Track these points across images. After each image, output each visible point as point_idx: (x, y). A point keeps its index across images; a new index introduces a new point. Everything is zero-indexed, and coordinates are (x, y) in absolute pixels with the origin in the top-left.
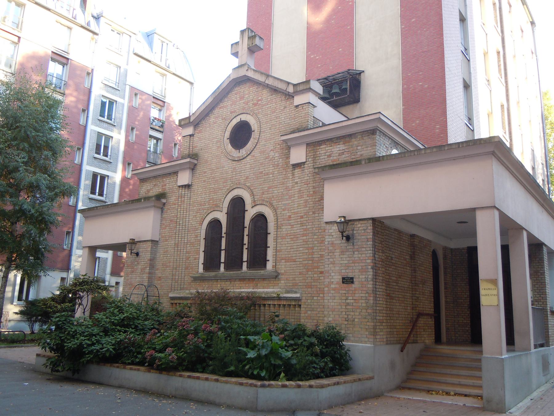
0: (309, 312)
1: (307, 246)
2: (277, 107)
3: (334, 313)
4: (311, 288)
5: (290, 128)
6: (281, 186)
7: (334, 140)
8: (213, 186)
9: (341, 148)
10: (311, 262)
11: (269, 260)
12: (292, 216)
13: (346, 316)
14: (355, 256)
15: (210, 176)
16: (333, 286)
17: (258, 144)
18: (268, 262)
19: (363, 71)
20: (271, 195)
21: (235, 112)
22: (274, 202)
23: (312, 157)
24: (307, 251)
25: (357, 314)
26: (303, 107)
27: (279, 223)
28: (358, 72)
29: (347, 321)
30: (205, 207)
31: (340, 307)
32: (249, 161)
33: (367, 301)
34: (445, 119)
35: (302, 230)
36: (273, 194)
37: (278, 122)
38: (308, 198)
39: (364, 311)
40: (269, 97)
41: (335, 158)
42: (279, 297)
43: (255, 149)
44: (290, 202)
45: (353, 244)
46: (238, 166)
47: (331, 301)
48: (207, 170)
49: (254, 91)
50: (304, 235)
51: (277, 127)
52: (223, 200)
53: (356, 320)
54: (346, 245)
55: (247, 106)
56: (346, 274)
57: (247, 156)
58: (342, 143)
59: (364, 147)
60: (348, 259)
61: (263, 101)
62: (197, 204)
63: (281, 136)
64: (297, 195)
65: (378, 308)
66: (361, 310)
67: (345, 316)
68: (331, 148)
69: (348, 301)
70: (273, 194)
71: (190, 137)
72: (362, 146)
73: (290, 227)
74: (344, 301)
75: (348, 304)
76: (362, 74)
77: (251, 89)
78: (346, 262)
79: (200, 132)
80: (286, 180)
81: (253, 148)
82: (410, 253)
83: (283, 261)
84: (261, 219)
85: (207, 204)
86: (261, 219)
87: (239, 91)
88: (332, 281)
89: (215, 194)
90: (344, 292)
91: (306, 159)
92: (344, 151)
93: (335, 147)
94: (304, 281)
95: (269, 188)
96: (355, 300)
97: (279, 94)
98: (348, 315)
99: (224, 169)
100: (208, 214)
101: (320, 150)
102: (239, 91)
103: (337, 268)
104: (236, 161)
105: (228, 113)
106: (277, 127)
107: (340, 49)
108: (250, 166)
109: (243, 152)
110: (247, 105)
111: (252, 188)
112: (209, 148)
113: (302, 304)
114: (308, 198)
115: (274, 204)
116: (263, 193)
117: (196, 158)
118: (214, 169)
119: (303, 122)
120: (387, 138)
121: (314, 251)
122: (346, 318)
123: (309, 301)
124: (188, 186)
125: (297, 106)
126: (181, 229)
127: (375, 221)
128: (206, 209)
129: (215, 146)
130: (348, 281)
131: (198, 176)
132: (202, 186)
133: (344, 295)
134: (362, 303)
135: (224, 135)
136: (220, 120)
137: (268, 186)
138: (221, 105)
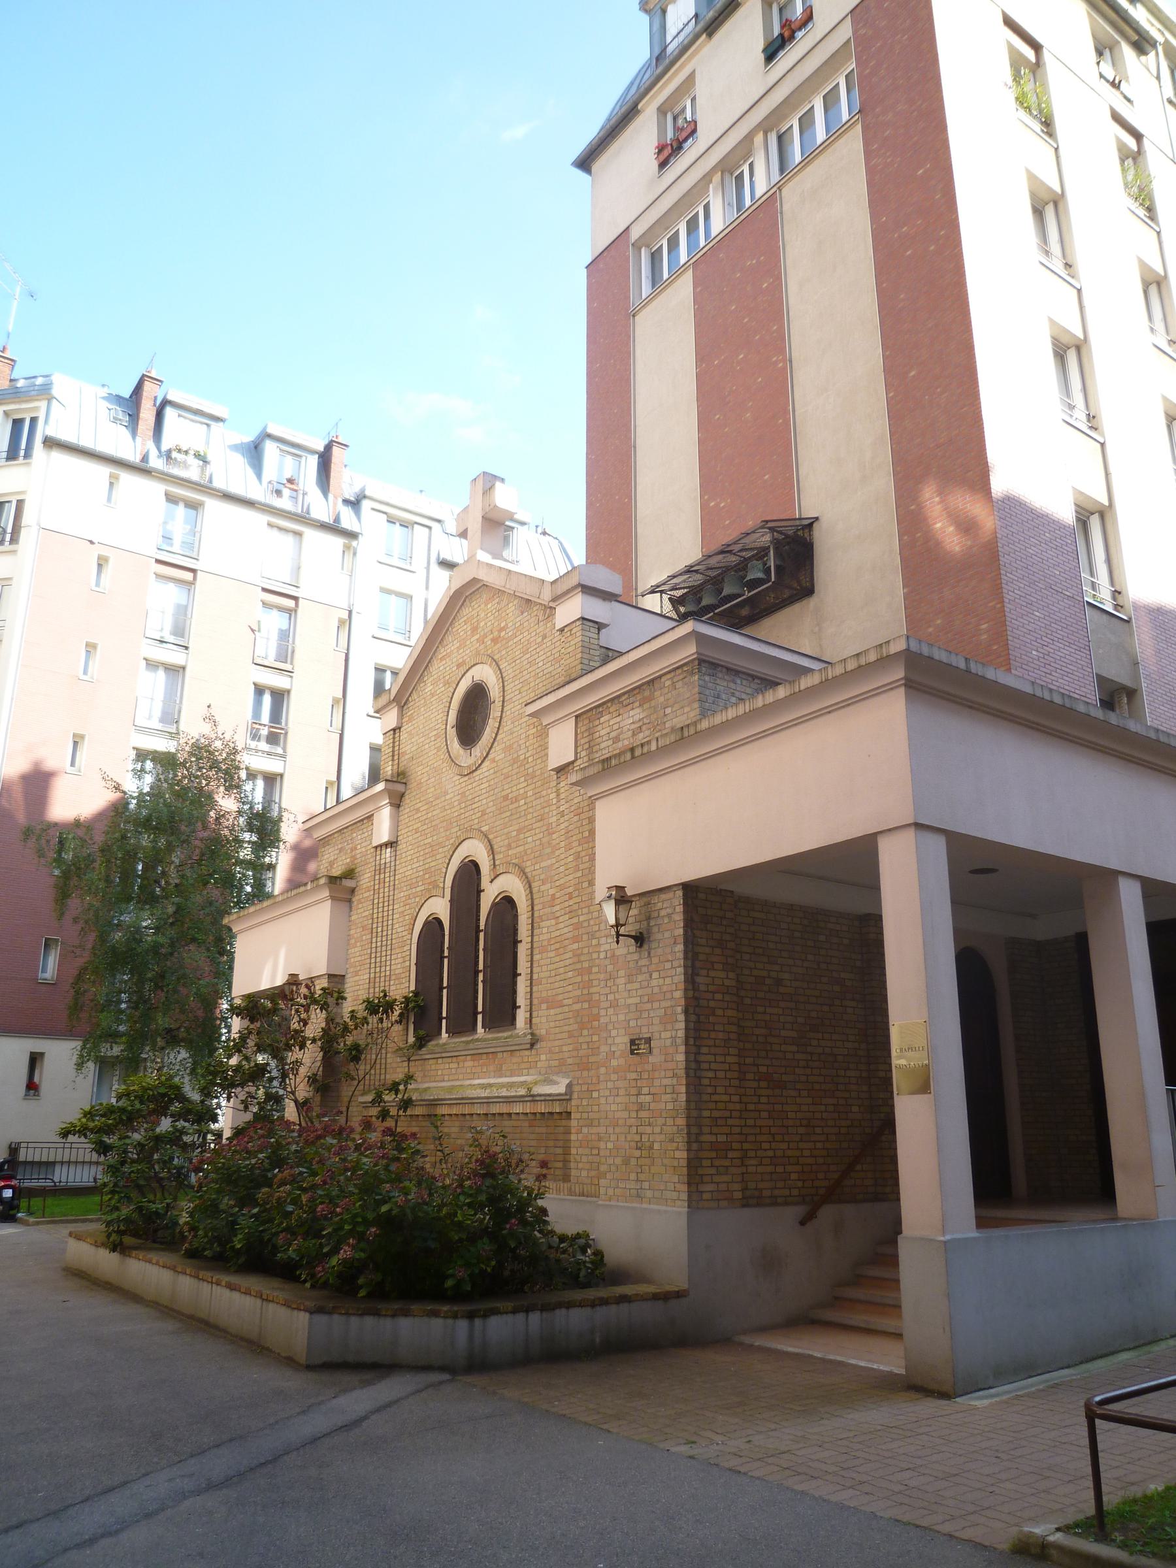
0: (585, 1130)
1: (579, 966)
2: (532, 640)
3: (617, 1130)
4: (588, 1070)
5: (553, 683)
6: (539, 824)
7: (624, 698)
8: (430, 840)
9: (637, 718)
10: (586, 1005)
11: (519, 1007)
12: (558, 895)
13: (637, 1138)
14: (654, 983)
15: (425, 817)
16: (614, 1063)
17: (500, 732)
18: (518, 1011)
19: (817, 519)
20: (521, 848)
21: (464, 663)
22: (529, 863)
23: (587, 746)
24: (579, 979)
25: (657, 1130)
26: (571, 630)
27: (536, 914)
28: (806, 522)
29: (640, 1149)
30: (418, 889)
31: (625, 1114)
32: (486, 774)
33: (675, 1096)
34: (999, 606)
35: (570, 928)
36: (527, 846)
37: (533, 674)
38: (580, 849)
39: (670, 1122)
40: (518, 619)
41: (626, 742)
42: (533, 1096)
43: (496, 744)
44: (554, 861)
45: (649, 953)
46: (470, 787)
47: (611, 1099)
48: (420, 805)
49: (494, 611)
50: (576, 939)
51: (532, 684)
52: (444, 870)
53: (656, 1146)
54: (636, 956)
55: (482, 646)
56: (638, 1031)
57: (482, 762)
58: (637, 704)
59: (676, 707)
60: (640, 992)
61: (508, 630)
62: (406, 884)
63: (526, 705)
64: (563, 844)
65: (706, 1113)
66: (663, 1122)
67: (635, 1136)
68: (618, 719)
69: (642, 1099)
70: (527, 846)
71: (394, 734)
72: (672, 706)
73: (553, 922)
74: (633, 1099)
75: (641, 1107)
76: (814, 525)
77: (489, 606)
78: (637, 1000)
79: (410, 721)
80: (547, 810)
81: (491, 741)
82: (858, 964)
83: (544, 1006)
84: (506, 904)
85: (420, 884)
86: (506, 904)
87: (470, 615)
88: (612, 1049)
89: (434, 858)
90: (634, 1075)
91: (576, 753)
92: (641, 723)
93: (625, 716)
94: (575, 1053)
95: (519, 831)
96: (653, 1094)
97: (535, 609)
98: (641, 1134)
99: (448, 797)
100: (422, 906)
101: (600, 727)
102: (470, 615)
103: (621, 1017)
104: (465, 775)
105: (454, 669)
106: (532, 684)
107: (767, 477)
108: (487, 785)
109: (478, 750)
110: (483, 643)
111: (491, 837)
112: (424, 753)
113: (573, 1110)
114: (580, 849)
115: (527, 870)
116: (509, 847)
117: (404, 781)
118: (431, 800)
119: (571, 665)
120: (744, 677)
121: (592, 977)
122: (637, 1142)
123: (585, 1102)
124: (391, 844)
125: (562, 630)
126: (379, 944)
127: (691, 890)
128: (419, 894)
129: (433, 748)
130: (638, 1045)
131: (407, 820)
132: (414, 842)
133: (633, 1083)
134: (666, 1102)
135: (447, 720)
136: (441, 688)
137: (516, 827)
138: (442, 652)
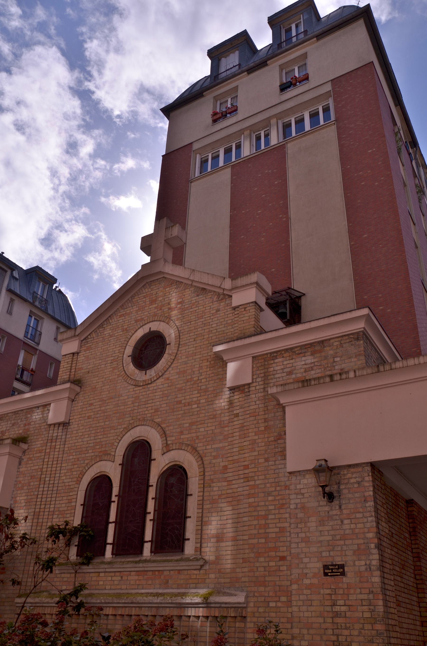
1: (256, 513)
2: (206, 311)
6: (211, 421)
7: (296, 349)
8: (103, 424)
9: (309, 361)
10: (263, 541)
12: (230, 466)
13: (334, 638)
16: (307, 582)
19: (304, 294)
21: (142, 319)
22: (199, 445)
23: (262, 375)
24: (256, 522)
25: (356, 633)
27: (207, 478)
28: (298, 294)
31: (321, 620)
33: (372, 607)
34: (418, 351)
36: (199, 434)
40: (193, 299)
41: (299, 375)
42: (207, 603)
43: (170, 369)
45: (340, 507)
46: (143, 393)
47: (304, 608)
50: (249, 496)
54: (327, 508)
55: (160, 311)
56: (330, 559)
58: (309, 353)
60: (332, 533)
61: (184, 304)
64: (237, 434)
66: (361, 626)
67: (332, 636)
68: (291, 361)
69: (337, 609)
70: (199, 434)
71: (73, 356)
73: (225, 484)
74: (329, 609)
75: (337, 615)
76: (302, 297)
77: (167, 289)
78: (330, 538)
79: (89, 349)
81: (167, 367)
89: (105, 436)
91: (253, 379)
92: (313, 365)
95: (191, 424)
96: (349, 606)
97: (209, 294)
98: (338, 636)
99: (122, 398)
101: (274, 365)
102: (149, 293)
104: (140, 386)
107: (273, 270)
109: (152, 373)
110: (161, 309)
111: (163, 426)
114: (256, 437)
115: (198, 449)
118: (105, 399)
121: (269, 521)
122: (334, 641)
123: (261, 610)
124: (65, 425)
125: (234, 308)
126: (46, 489)
129: (110, 367)
133: (328, 597)
134: (363, 612)
